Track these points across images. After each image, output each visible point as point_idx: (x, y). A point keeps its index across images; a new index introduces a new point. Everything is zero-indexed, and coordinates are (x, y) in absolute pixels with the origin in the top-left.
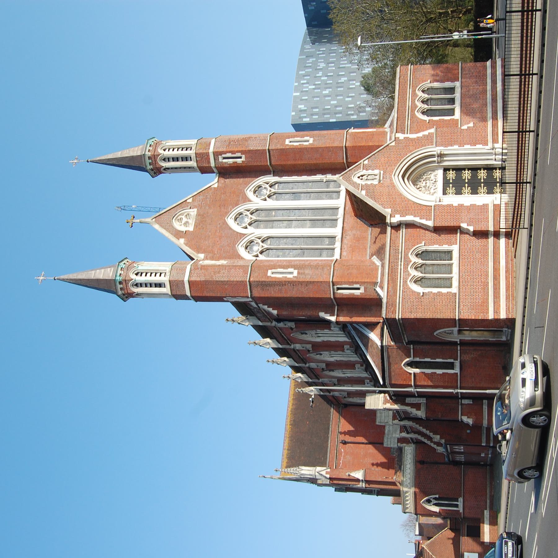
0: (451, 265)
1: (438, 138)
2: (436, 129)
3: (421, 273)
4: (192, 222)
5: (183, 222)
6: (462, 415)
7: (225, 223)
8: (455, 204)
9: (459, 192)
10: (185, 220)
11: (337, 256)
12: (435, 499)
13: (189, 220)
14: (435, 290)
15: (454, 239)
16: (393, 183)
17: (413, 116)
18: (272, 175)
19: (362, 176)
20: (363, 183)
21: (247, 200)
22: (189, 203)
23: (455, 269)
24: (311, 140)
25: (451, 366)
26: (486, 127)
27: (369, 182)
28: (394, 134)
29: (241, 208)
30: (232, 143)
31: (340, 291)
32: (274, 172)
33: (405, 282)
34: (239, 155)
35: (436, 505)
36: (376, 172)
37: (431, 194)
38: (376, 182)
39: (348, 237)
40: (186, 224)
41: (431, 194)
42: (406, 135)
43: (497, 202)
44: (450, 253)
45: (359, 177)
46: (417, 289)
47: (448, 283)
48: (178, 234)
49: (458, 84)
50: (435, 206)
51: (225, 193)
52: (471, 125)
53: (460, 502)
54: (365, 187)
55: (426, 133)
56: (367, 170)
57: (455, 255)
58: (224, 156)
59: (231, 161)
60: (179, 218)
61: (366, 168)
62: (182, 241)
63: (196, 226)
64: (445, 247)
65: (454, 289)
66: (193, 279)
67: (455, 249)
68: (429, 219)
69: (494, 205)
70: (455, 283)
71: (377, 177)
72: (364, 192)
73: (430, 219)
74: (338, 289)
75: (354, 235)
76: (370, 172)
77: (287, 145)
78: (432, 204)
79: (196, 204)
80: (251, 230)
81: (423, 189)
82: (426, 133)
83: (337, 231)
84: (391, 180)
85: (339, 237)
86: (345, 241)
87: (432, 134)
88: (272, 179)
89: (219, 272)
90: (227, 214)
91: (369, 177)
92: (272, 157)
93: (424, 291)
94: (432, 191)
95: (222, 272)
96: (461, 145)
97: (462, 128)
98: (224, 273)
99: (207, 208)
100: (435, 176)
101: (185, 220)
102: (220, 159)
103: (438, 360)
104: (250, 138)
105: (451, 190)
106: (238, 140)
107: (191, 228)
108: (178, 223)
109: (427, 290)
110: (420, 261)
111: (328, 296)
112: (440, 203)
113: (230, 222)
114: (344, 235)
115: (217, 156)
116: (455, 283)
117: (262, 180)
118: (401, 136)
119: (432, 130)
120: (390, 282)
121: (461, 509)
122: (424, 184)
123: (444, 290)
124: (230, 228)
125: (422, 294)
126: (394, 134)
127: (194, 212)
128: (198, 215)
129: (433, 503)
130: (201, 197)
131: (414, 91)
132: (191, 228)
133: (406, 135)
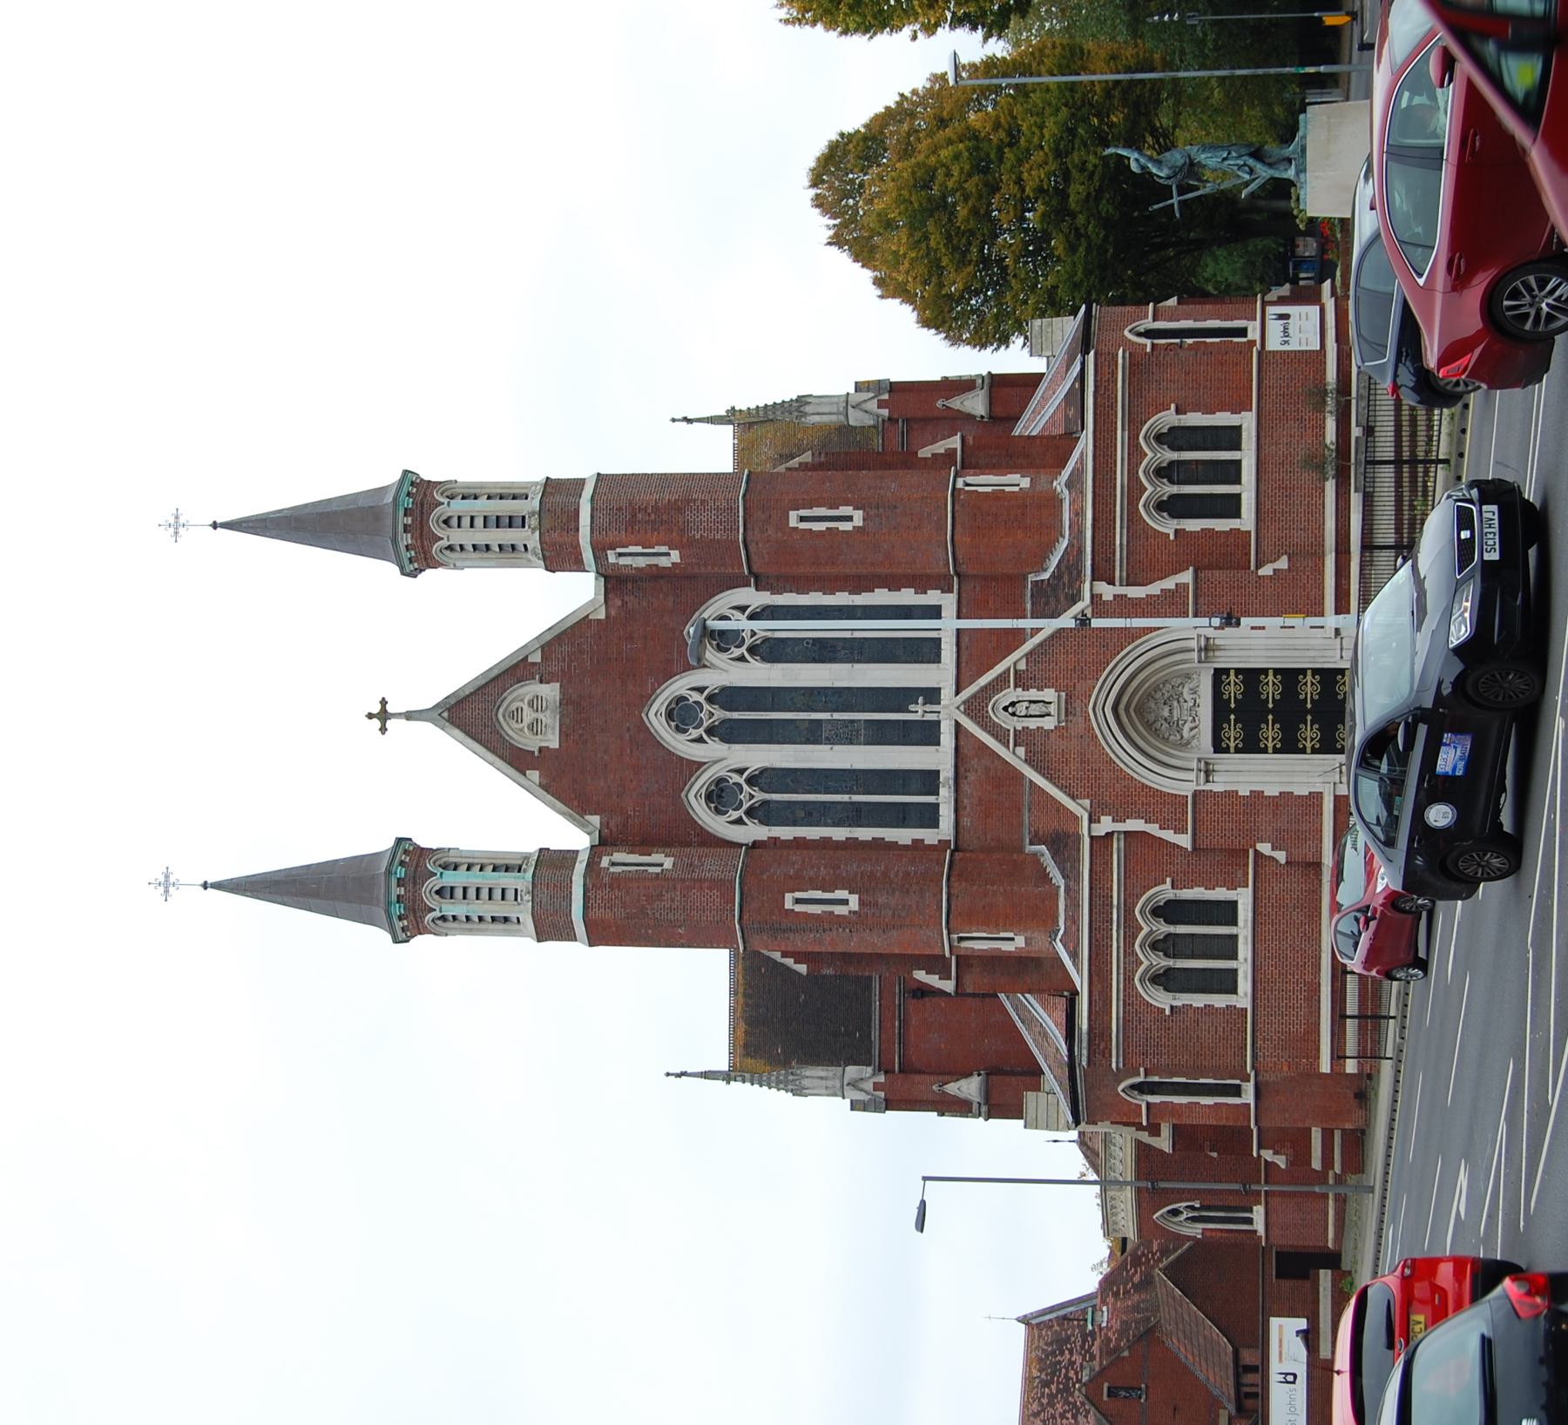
0: (1234, 938)
1: (1201, 600)
2: (1196, 572)
3: (1166, 955)
4: (551, 720)
5: (527, 720)
6: (1260, 1147)
7: (643, 728)
8: (1244, 791)
9: (1251, 745)
10: (529, 715)
11: (946, 828)
12: (1192, 1208)
13: (540, 716)
14: (1198, 1000)
15: (1240, 873)
16: (1090, 729)
17: (1133, 517)
18: (752, 589)
19: (1013, 704)
20: (1019, 728)
22: (534, 664)
23: (1245, 950)
25: (1236, 1091)
26: (1322, 573)
27: (1033, 724)
28: (1087, 585)
29: (680, 686)
30: (640, 516)
31: (965, 944)
32: (757, 578)
33: (1129, 980)
34: (664, 549)
35: (1194, 1219)
36: (1049, 694)
38: (1049, 724)
39: (971, 777)
42: (1119, 590)
43: (1343, 790)
44: (1233, 905)
45: (1005, 709)
47: (1226, 982)
49: (1247, 421)
50: (1196, 794)
51: (630, 638)
52: (1283, 563)
53: (1258, 1214)
54: (1022, 737)
55: (1169, 583)
56: (1026, 688)
57: (1245, 913)
58: (619, 550)
59: (641, 562)
60: (513, 707)
61: (1022, 681)
63: (564, 735)
64: (1221, 894)
65: (1243, 997)
66: (597, 914)
67: (1244, 898)
68: (1181, 830)
69: (1336, 797)
70: (1244, 985)
71: (1053, 709)
72: (1021, 751)
73: (1184, 831)
74: (961, 939)
75: (987, 769)
76: (1033, 694)
78: (1187, 789)
79: (554, 668)
80: (714, 749)
81: (1165, 725)
82: (1169, 583)
83: (939, 759)
84: (1087, 719)
85: (947, 773)
86: (966, 788)
87: (1186, 586)
89: (660, 897)
90: (646, 699)
92: (754, 557)
93: (1175, 1003)
94: (1186, 733)
95: (667, 896)
97: (1261, 572)
98: (672, 900)
99: (587, 681)
100: (1194, 691)
101: (529, 715)
102: (612, 558)
103: (1202, 1081)
104: (688, 501)
105: (1233, 733)
106: (656, 509)
108: (515, 725)
110: (1164, 929)
111: (937, 952)
112: (1208, 787)
113: (656, 719)
114: (962, 770)
115: (604, 550)
116: (1244, 985)
118: (1107, 591)
119: (1187, 577)
120: (1095, 978)
121: (1259, 1225)
122: (1166, 714)
123: (1219, 1001)
125: (1168, 1012)
126: (1087, 585)
128: (565, 701)
129: (1185, 1216)
130: (566, 649)
133: (1119, 590)
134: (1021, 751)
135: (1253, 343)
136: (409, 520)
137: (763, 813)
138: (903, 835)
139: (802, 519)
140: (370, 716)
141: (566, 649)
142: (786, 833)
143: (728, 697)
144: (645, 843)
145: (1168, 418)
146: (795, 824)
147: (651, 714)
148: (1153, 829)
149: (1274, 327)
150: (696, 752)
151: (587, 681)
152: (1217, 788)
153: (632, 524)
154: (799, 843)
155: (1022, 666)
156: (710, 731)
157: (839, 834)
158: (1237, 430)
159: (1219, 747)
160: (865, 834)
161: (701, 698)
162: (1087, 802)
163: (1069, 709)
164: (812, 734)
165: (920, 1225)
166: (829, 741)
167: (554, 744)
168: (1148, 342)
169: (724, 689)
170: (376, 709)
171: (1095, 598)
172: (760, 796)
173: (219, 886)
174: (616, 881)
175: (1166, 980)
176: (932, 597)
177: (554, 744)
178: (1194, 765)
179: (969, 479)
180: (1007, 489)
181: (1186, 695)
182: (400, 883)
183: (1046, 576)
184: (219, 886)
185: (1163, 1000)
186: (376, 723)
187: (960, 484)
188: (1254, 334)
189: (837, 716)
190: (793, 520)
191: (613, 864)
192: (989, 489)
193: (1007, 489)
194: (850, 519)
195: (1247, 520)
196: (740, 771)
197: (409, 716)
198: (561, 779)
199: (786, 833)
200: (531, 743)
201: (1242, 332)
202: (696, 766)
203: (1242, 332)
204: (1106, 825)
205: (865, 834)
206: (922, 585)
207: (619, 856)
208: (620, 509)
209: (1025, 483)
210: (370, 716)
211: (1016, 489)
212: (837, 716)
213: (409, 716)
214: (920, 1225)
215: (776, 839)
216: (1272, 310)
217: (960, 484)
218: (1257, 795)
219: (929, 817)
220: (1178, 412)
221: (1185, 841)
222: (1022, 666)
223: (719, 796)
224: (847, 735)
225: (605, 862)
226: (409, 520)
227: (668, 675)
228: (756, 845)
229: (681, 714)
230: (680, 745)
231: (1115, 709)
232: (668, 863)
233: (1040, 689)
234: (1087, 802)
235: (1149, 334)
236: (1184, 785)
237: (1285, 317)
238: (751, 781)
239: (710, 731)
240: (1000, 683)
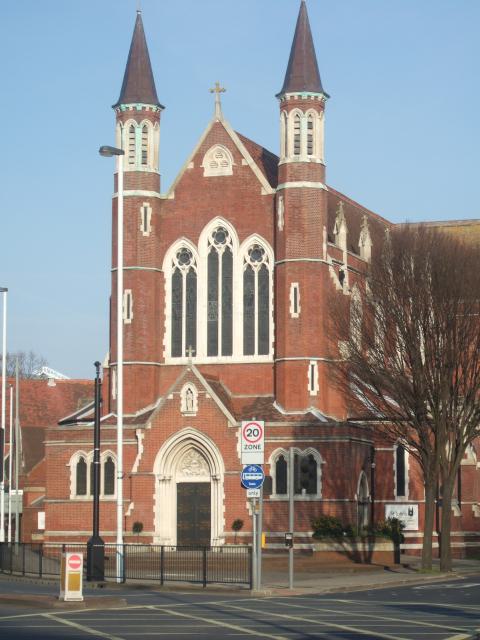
5: (216, 160)
8: (155, 497)
14: (73, 478)
21: (242, 238)
24: (295, 315)
27: (183, 402)
29: (232, 233)
30: (297, 211)
33: (80, 448)
36: (196, 409)
37: (172, 470)
40: (214, 165)
41: (172, 470)
48: (198, 159)
54: (177, 399)
56: (198, 398)
61: (201, 397)
62: (191, 166)
63: (210, 179)
72: (171, 397)
76: (196, 402)
77: (290, 286)
79: (240, 172)
88: (271, 267)
90: (226, 216)
91: (190, 402)
96: (225, 502)
100: (203, 474)
101: (219, 161)
107: (207, 174)
112: (157, 481)
113: (216, 223)
116: (80, 498)
117: (269, 252)
123: (73, 487)
124: (205, 224)
127: (228, 171)
128: (223, 178)
130: (248, 177)
132: (207, 174)
134: (171, 397)
135: (393, 498)
136: (296, 98)
137: (177, 276)
138: (167, 340)
139: (295, 289)
140: (217, 85)
141: (248, 177)
142: (168, 287)
143: (228, 255)
144: (157, 221)
145: (319, 459)
146: (173, 291)
147: (219, 220)
148: (139, 457)
149: (405, 508)
151: (234, 188)
152: (157, 485)
153: (294, 207)
155: (208, 396)
156: (213, 249)
157: (168, 311)
158: (315, 492)
159: (180, 486)
160: (168, 324)
161: (228, 243)
162: (149, 427)
163: (189, 421)
164: (212, 296)
166: (209, 304)
167: (206, 174)
169: (231, 254)
170: (221, 87)
171: (236, 429)
172: (184, 274)
173: (139, 18)
174: (138, 210)
175: (82, 465)
176: (272, 351)
177: (206, 174)
180: (309, 386)
181: (202, 470)
182: (135, 108)
183: (275, 405)
184: (139, 18)
185: (74, 462)
186: (214, 87)
187: (312, 363)
188: (398, 499)
189: (220, 308)
190: (295, 285)
191: (146, 209)
192: (309, 376)
193: (309, 386)
194: (296, 311)
196: (195, 264)
198: (192, 181)
200: (206, 163)
202: (196, 244)
203: (401, 492)
204: (140, 436)
206: (275, 345)
207: (150, 210)
208: (300, 201)
209: (313, 393)
210: (217, 85)
211: (309, 388)
212: (220, 308)
215: (164, 282)
216: (415, 508)
218: (153, 502)
219: (176, 352)
221: (135, 470)
222: (208, 396)
223: (185, 256)
224: (212, 314)
225: (146, 204)
226: (296, 98)
227: (237, 226)
228: (162, 274)
229: (220, 236)
230: (207, 234)
231: (190, 439)
233: (198, 405)
234: (149, 427)
238: (192, 269)
239: (213, 249)
240: (200, 387)
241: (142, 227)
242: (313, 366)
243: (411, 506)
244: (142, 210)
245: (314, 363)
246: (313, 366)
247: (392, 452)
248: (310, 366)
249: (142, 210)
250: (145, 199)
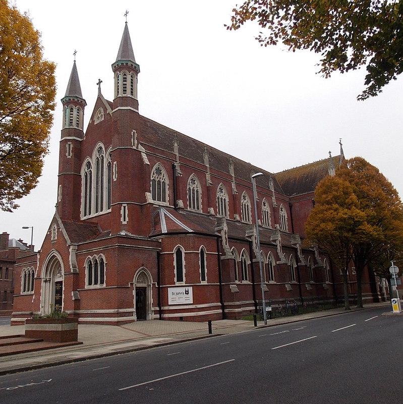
46: (23, 275)
109: (23, 279)
123: (22, 288)
128: (101, 123)
131: (101, 252)
149: (183, 290)
150: (94, 157)
152: (43, 284)
154: (80, 185)
165: (23, 228)
168: (174, 251)
173: (75, 64)
178: (48, 277)
179: (126, 207)
187: (123, 205)
188: (177, 284)
195: (87, 287)
197: (99, 89)
199: (83, 182)
200: (95, 119)
201: (180, 279)
203: (180, 279)
204: (38, 257)
205: (83, 200)
213: (99, 89)
214: (23, 228)
216: (190, 289)
217: (123, 205)
220: (106, 264)
232: (70, 157)
235: (179, 253)
236: (43, 276)
237: (187, 292)
241: (67, 154)
242: (125, 207)
243: (187, 288)
244: (67, 146)
245: (126, 205)
246: (125, 207)
247: (173, 253)
248: (122, 208)
249: (67, 146)
250: (69, 140)
